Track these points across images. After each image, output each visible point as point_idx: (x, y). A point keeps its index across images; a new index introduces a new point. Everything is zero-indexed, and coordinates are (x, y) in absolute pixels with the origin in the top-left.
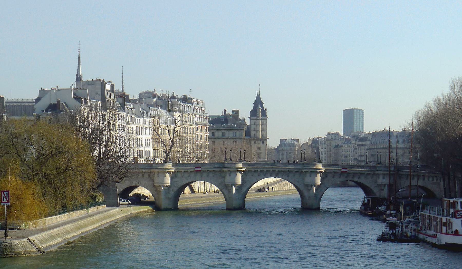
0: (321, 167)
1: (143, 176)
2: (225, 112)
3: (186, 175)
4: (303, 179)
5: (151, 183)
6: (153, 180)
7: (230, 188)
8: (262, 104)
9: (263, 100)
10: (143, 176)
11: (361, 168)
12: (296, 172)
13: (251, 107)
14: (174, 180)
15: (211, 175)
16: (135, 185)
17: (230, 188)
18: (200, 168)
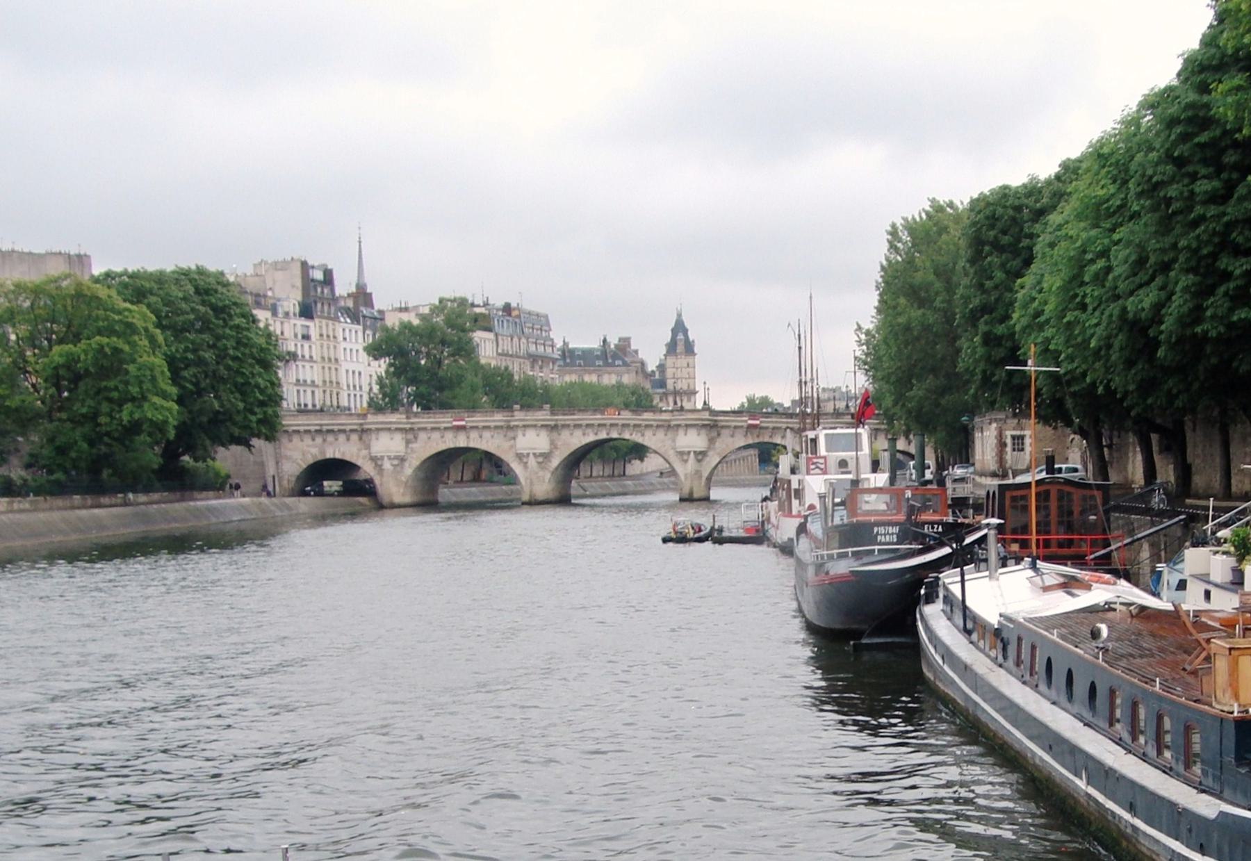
0: (708, 417)
1: (348, 439)
2: (605, 341)
3: (436, 435)
4: (674, 441)
5: (364, 452)
6: (368, 447)
7: (525, 460)
8: (685, 331)
9: (687, 325)
10: (348, 439)
11: (787, 418)
12: (658, 426)
13: (668, 337)
14: (410, 445)
15: (487, 434)
16: (332, 456)
17: (525, 460)
18: (463, 420)
